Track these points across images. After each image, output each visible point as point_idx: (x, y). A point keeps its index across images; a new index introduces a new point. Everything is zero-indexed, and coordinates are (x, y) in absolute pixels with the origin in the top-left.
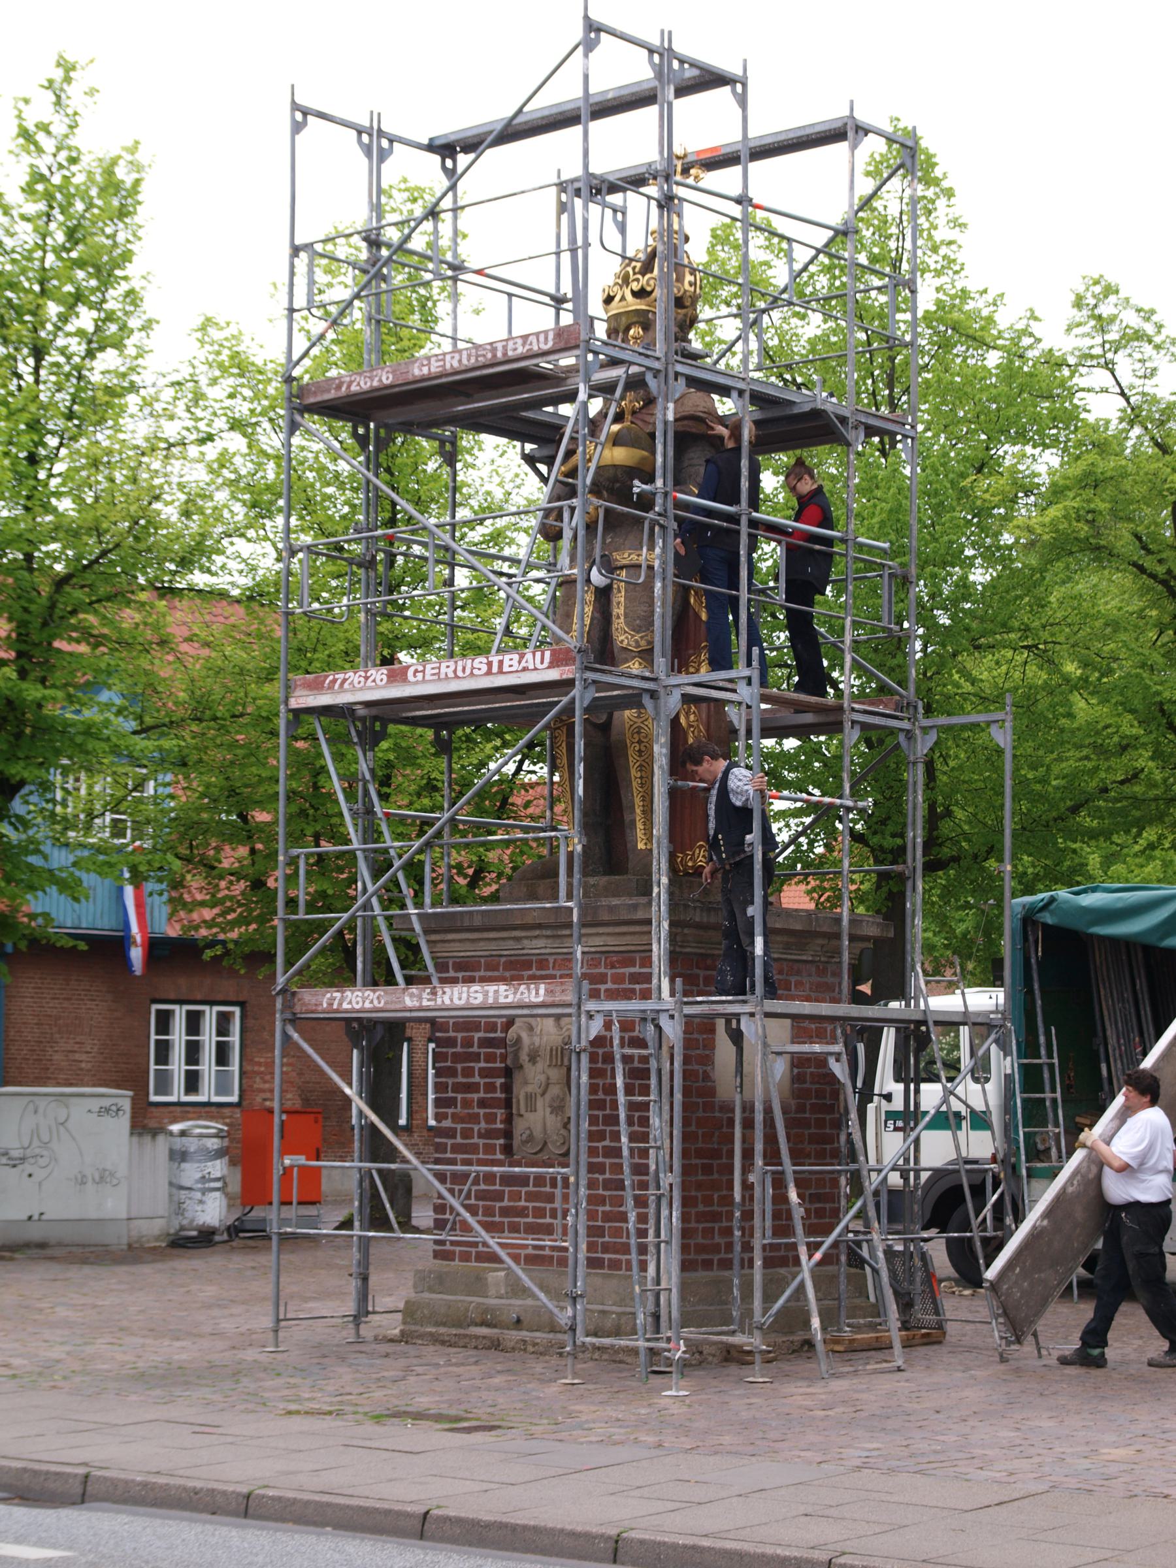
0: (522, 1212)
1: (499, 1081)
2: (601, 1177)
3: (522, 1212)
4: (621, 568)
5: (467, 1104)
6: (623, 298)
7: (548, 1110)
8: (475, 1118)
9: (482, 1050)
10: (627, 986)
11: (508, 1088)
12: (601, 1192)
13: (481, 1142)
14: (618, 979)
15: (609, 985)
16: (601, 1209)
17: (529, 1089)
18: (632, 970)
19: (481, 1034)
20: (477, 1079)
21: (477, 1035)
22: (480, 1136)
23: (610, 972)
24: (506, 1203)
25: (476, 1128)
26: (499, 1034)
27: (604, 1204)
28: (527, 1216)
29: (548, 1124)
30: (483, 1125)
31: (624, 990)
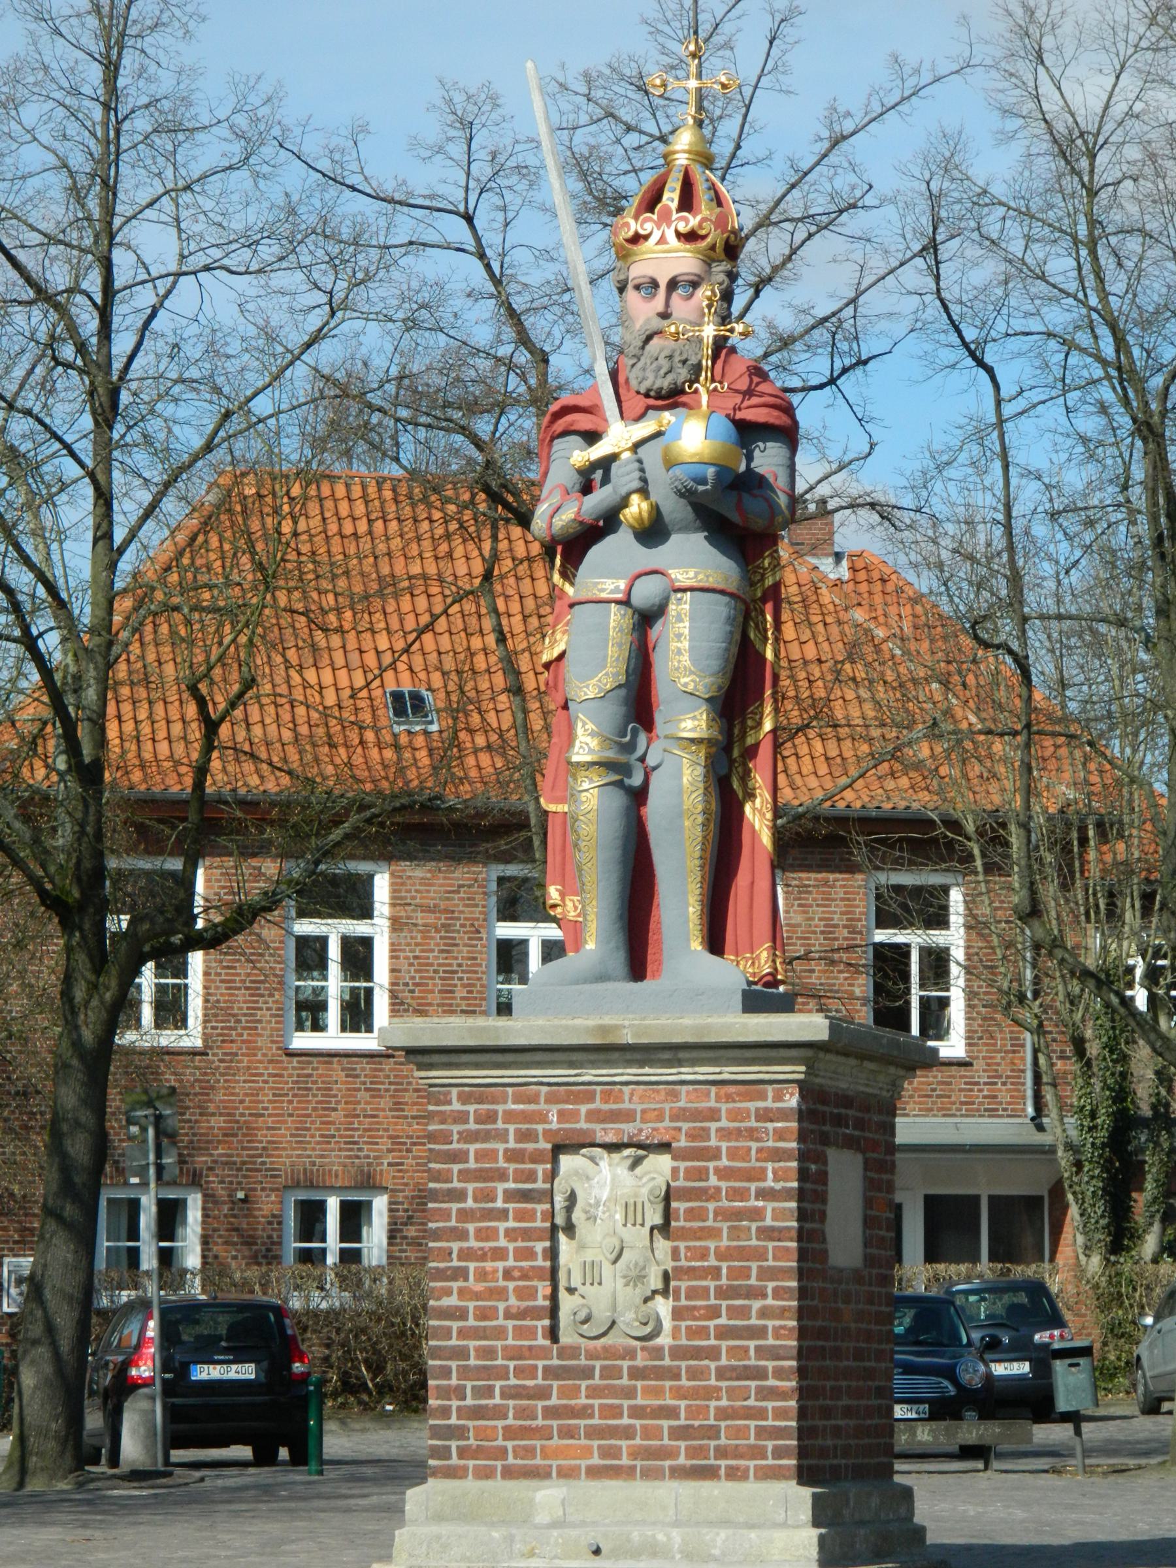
0: (584, 1412)
1: (540, 1246)
2: (713, 1365)
3: (584, 1412)
4: (684, 590)
5: (482, 1275)
6: (662, 240)
7: (620, 1282)
8: (501, 1294)
9: (511, 1206)
10: (753, 1123)
11: (553, 1254)
12: (713, 1382)
13: (510, 1324)
14: (735, 1115)
15: (724, 1123)
16: (713, 1404)
17: (589, 1255)
18: (761, 1104)
19: (511, 1185)
20: (502, 1242)
21: (501, 1187)
22: (508, 1315)
23: (724, 1107)
24: (554, 1401)
25: (501, 1306)
26: (540, 1185)
27: (718, 1399)
28: (591, 1416)
29: (620, 1300)
30: (513, 1301)
31: (751, 1131)
